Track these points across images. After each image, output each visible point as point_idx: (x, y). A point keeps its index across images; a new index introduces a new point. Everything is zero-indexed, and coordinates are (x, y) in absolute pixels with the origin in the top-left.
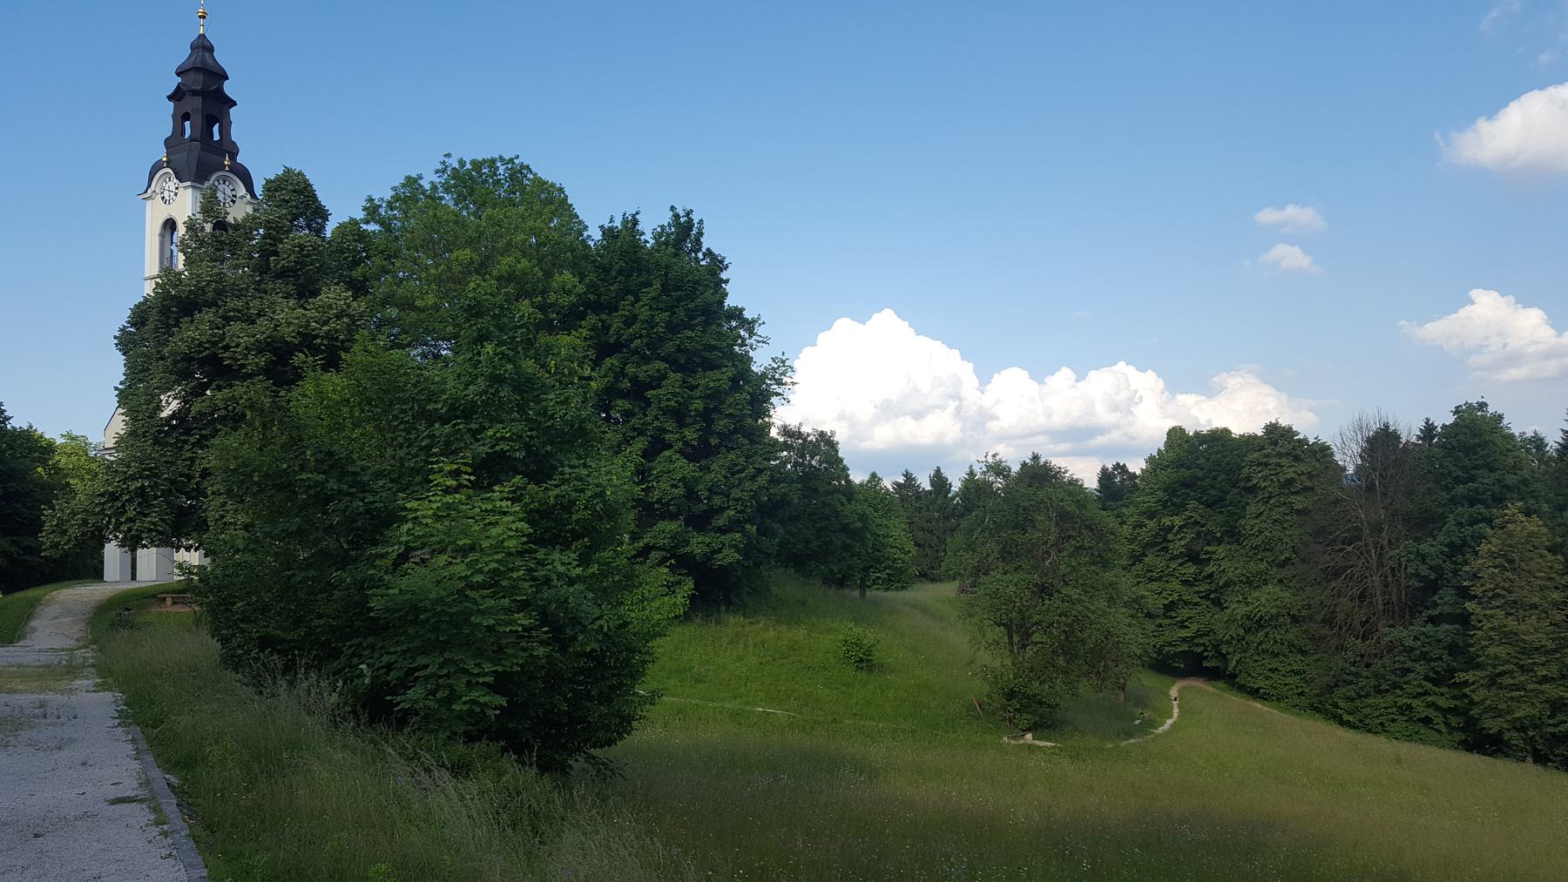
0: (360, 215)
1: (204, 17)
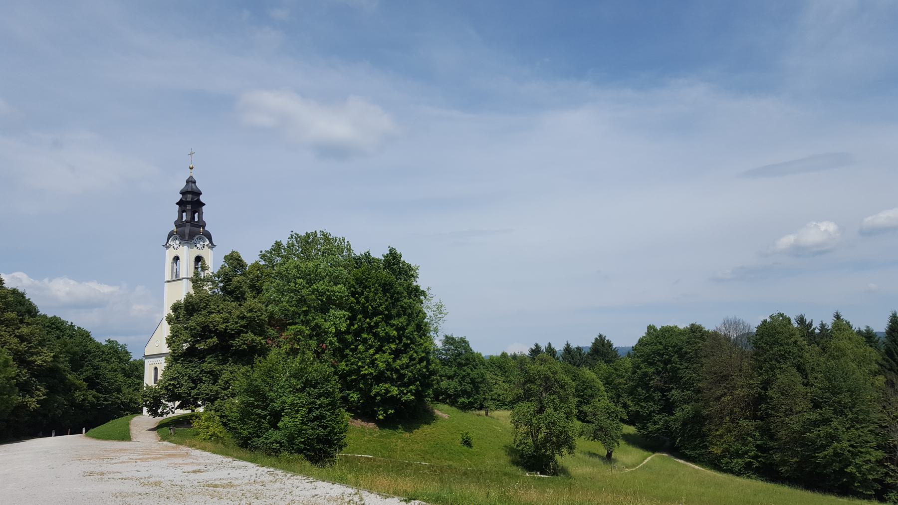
0: (258, 258)
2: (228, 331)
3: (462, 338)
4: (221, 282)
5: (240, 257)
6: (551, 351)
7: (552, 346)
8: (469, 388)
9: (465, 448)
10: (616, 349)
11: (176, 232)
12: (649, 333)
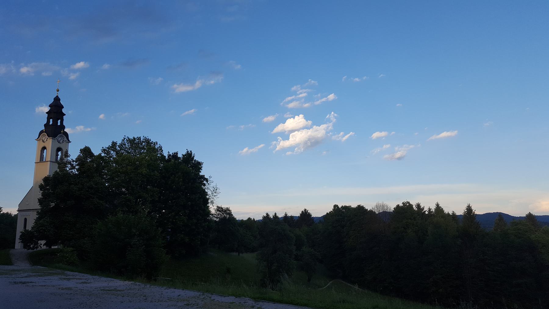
0: (100, 152)
1: (58, 91)
3: (227, 208)
4: (77, 165)
6: (275, 216)
7: (277, 215)
10: (313, 218)
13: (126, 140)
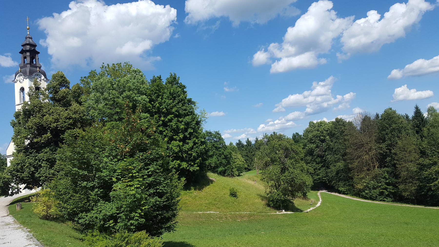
0: (79, 82)
1: (29, 29)
2: (58, 128)
5: (64, 75)
6: (249, 142)
8: (224, 161)
9: (233, 198)
11: (21, 71)
12: (310, 126)
13: (104, 67)
